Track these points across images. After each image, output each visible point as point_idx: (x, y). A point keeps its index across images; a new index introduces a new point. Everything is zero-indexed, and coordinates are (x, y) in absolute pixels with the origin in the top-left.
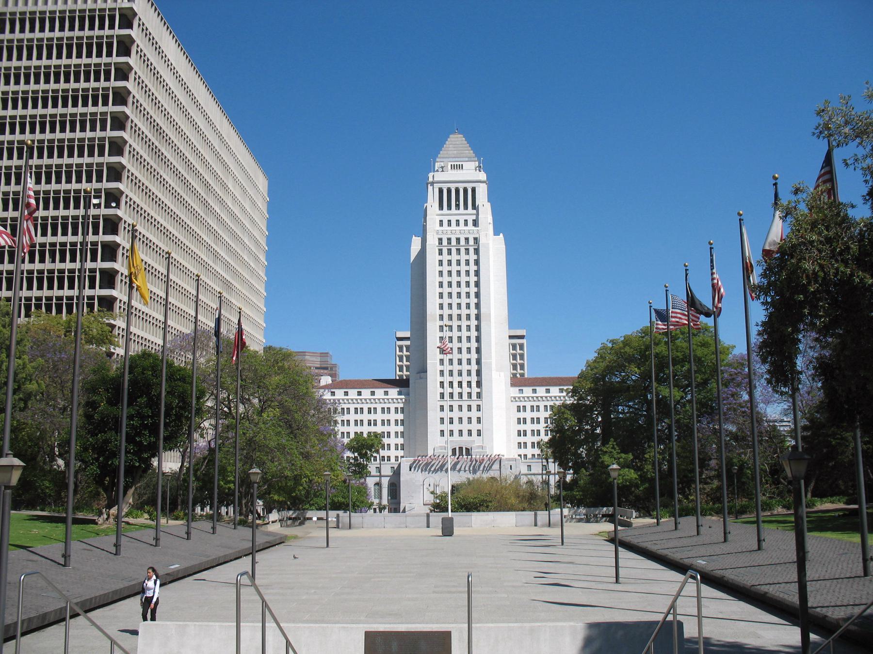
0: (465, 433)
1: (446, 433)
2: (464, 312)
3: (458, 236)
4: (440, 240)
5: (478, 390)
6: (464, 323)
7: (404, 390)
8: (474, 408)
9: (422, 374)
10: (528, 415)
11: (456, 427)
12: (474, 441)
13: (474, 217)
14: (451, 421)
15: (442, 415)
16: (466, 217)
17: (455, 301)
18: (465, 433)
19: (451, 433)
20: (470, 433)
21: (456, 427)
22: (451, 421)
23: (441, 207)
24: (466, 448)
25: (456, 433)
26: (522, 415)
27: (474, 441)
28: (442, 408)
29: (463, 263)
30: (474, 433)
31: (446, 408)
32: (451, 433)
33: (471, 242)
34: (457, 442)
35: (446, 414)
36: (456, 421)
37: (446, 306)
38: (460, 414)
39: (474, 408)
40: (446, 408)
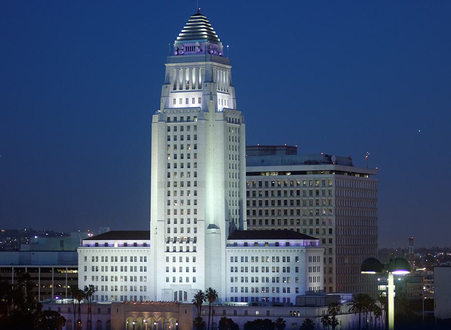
0: (184, 280)
1: (171, 280)
5: (194, 245)
7: (147, 242)
8: (191, 260)
10: (239, 265)
15: (167, 264)
18: (184, 280)
24: (185, 292)
25: (177, 280)
26: (234, 264)
30: (191, 280)
31: (171, 259)
38: (181, 264)
39: (191, 260)
40: (171, 259)
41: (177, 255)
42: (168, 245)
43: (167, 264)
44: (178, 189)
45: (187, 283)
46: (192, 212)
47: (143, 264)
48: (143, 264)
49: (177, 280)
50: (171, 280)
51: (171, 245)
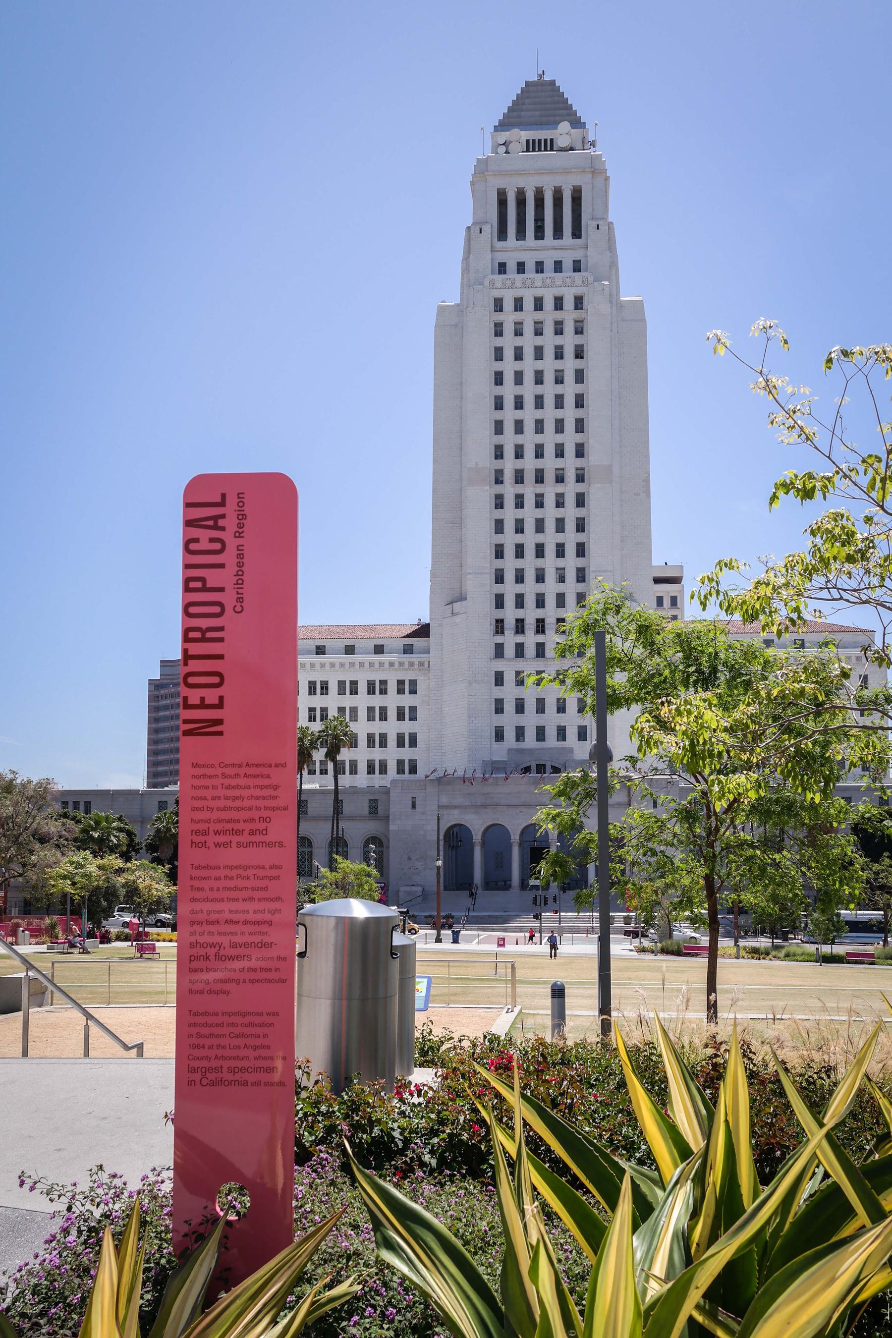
1: (510, 735)
2: (550, 463)
3: (539, 293)
4: (498, 305)
6: (550, 490)
9: (457, 606)
11: (531, 720)
12: (571, 750)
13: (578, 255)
14: (520, 707)
15: (498, 692)
16: (557, 255)
17: (529, 439)
18: (551, 733)
19: (520, 733)
20: (562, 733)
21: (531, 720)
22: (520, 707)
23: (502, 234)
25: (530, 734)
27: (571, 750)
28: (499, 679)
29: (549, 353)
31: (509, 678)
32: (520, 733)
33: (569, 303)
34: (531, 751)
35: (509, 692)
36: (530, 706)
37: (509, 452)
41: (529, 666)
42: (499, 639)
43: (498, 692)
44: (529, 490)
45: (561, 744)
46: (571, 550)
47: (407, 700)
48: (407, 700)
49: (530, 734)
50: (510, 735)
51: (510, 639)
